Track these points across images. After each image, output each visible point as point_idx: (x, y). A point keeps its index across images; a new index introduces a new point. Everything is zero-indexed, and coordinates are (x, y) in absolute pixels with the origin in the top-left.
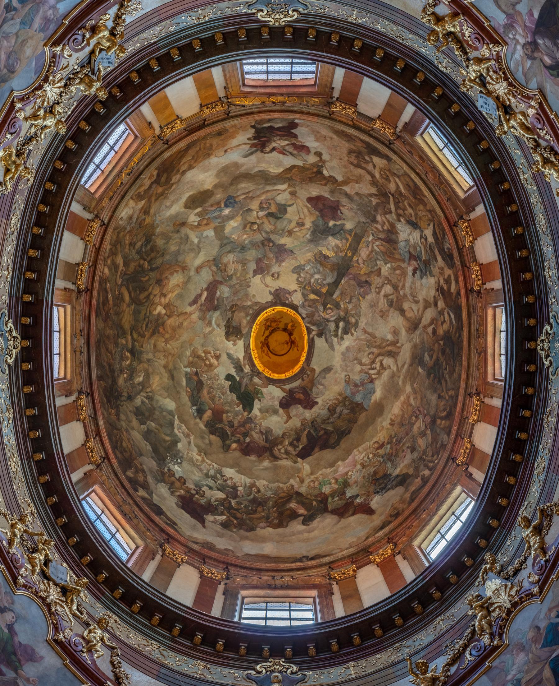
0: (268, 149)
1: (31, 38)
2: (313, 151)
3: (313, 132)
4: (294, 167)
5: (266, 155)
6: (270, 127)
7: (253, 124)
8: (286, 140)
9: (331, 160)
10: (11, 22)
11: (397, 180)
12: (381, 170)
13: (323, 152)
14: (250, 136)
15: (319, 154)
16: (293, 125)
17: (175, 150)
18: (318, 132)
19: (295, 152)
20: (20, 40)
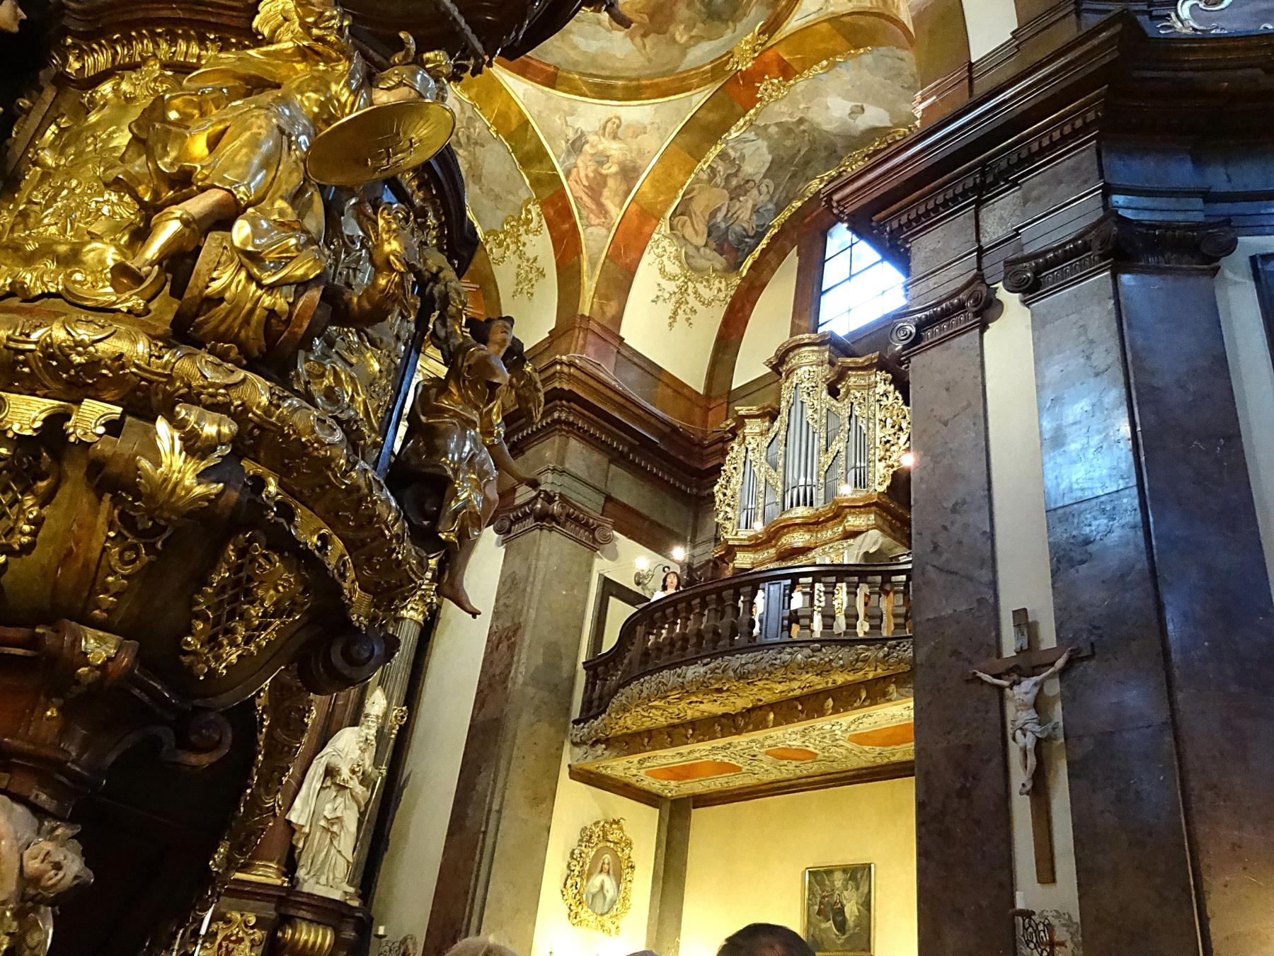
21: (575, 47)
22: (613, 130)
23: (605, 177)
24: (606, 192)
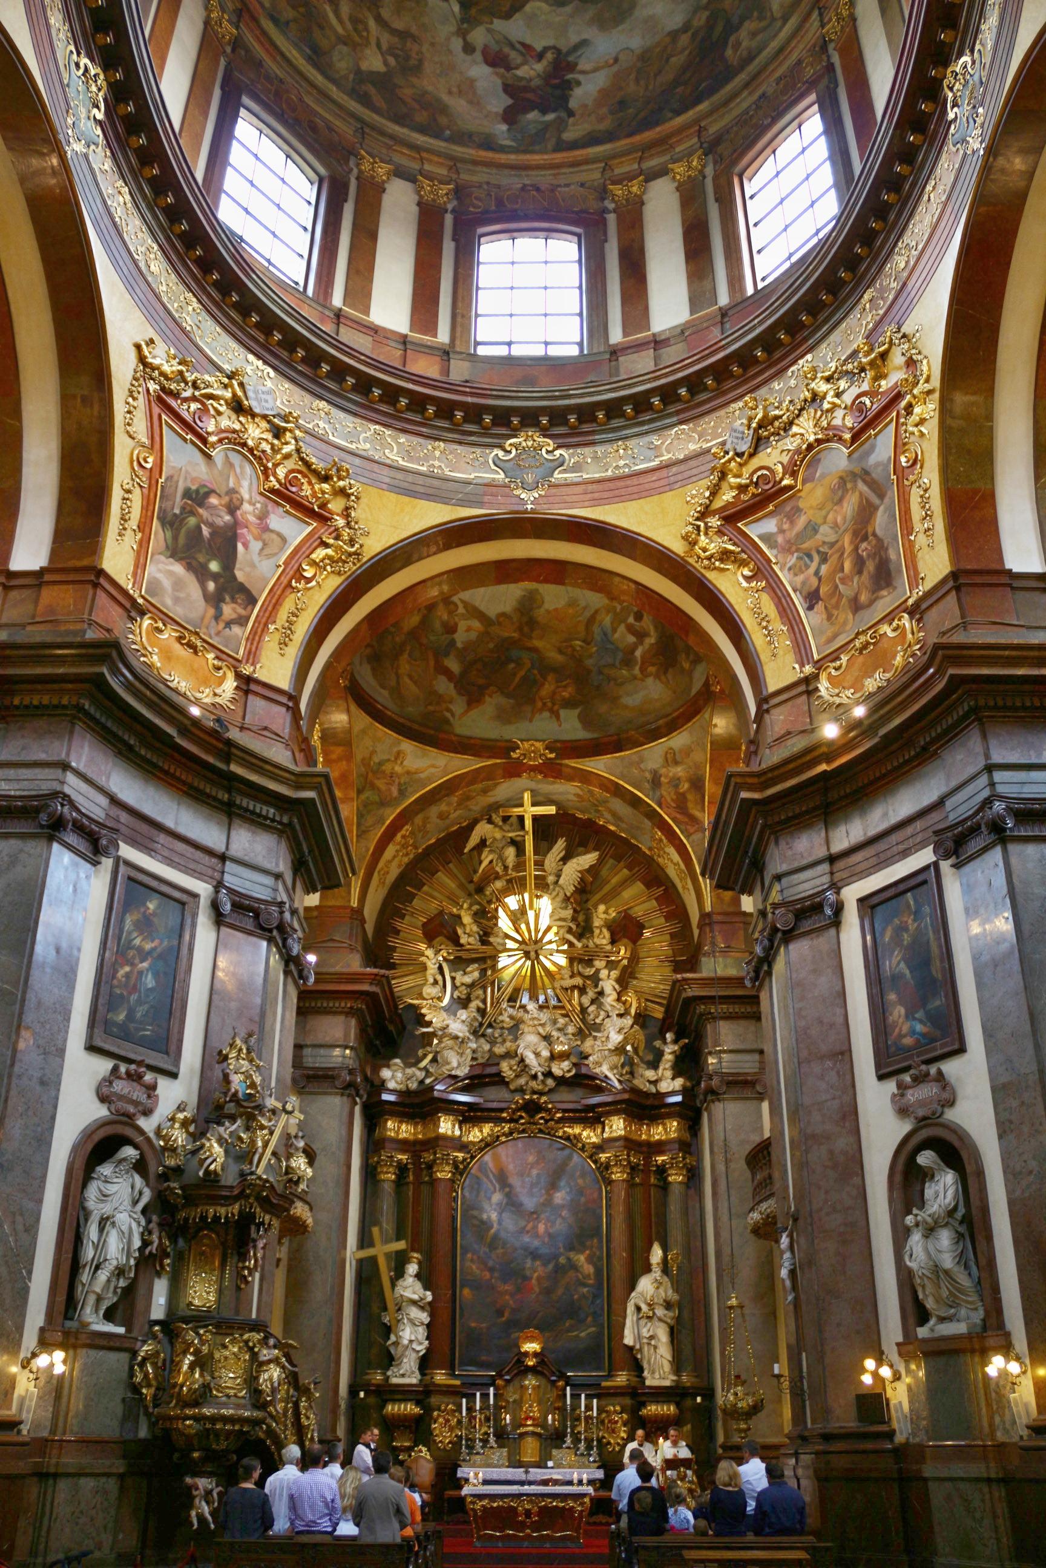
0: (550, 56)
1: (811, 507)
2: (478, 56)
3: (478, 103)
4: (508, 16)
5: (550, 42)
6: (544, 112)
7: (571, 120)
8: (522, 79)
9: (448, 39)
10: (827, 540)
11: (340, 30)
12: (367, 43)
13: (462, 55)
14: (578, 92)
15: (468, 49)
16: (510, 116)
17: (691, 113)
18: (471, 102)
19: (506, 50)
21: (626, 707)
22: (671, 758)
23: (683, 795)
24: (690, 805)
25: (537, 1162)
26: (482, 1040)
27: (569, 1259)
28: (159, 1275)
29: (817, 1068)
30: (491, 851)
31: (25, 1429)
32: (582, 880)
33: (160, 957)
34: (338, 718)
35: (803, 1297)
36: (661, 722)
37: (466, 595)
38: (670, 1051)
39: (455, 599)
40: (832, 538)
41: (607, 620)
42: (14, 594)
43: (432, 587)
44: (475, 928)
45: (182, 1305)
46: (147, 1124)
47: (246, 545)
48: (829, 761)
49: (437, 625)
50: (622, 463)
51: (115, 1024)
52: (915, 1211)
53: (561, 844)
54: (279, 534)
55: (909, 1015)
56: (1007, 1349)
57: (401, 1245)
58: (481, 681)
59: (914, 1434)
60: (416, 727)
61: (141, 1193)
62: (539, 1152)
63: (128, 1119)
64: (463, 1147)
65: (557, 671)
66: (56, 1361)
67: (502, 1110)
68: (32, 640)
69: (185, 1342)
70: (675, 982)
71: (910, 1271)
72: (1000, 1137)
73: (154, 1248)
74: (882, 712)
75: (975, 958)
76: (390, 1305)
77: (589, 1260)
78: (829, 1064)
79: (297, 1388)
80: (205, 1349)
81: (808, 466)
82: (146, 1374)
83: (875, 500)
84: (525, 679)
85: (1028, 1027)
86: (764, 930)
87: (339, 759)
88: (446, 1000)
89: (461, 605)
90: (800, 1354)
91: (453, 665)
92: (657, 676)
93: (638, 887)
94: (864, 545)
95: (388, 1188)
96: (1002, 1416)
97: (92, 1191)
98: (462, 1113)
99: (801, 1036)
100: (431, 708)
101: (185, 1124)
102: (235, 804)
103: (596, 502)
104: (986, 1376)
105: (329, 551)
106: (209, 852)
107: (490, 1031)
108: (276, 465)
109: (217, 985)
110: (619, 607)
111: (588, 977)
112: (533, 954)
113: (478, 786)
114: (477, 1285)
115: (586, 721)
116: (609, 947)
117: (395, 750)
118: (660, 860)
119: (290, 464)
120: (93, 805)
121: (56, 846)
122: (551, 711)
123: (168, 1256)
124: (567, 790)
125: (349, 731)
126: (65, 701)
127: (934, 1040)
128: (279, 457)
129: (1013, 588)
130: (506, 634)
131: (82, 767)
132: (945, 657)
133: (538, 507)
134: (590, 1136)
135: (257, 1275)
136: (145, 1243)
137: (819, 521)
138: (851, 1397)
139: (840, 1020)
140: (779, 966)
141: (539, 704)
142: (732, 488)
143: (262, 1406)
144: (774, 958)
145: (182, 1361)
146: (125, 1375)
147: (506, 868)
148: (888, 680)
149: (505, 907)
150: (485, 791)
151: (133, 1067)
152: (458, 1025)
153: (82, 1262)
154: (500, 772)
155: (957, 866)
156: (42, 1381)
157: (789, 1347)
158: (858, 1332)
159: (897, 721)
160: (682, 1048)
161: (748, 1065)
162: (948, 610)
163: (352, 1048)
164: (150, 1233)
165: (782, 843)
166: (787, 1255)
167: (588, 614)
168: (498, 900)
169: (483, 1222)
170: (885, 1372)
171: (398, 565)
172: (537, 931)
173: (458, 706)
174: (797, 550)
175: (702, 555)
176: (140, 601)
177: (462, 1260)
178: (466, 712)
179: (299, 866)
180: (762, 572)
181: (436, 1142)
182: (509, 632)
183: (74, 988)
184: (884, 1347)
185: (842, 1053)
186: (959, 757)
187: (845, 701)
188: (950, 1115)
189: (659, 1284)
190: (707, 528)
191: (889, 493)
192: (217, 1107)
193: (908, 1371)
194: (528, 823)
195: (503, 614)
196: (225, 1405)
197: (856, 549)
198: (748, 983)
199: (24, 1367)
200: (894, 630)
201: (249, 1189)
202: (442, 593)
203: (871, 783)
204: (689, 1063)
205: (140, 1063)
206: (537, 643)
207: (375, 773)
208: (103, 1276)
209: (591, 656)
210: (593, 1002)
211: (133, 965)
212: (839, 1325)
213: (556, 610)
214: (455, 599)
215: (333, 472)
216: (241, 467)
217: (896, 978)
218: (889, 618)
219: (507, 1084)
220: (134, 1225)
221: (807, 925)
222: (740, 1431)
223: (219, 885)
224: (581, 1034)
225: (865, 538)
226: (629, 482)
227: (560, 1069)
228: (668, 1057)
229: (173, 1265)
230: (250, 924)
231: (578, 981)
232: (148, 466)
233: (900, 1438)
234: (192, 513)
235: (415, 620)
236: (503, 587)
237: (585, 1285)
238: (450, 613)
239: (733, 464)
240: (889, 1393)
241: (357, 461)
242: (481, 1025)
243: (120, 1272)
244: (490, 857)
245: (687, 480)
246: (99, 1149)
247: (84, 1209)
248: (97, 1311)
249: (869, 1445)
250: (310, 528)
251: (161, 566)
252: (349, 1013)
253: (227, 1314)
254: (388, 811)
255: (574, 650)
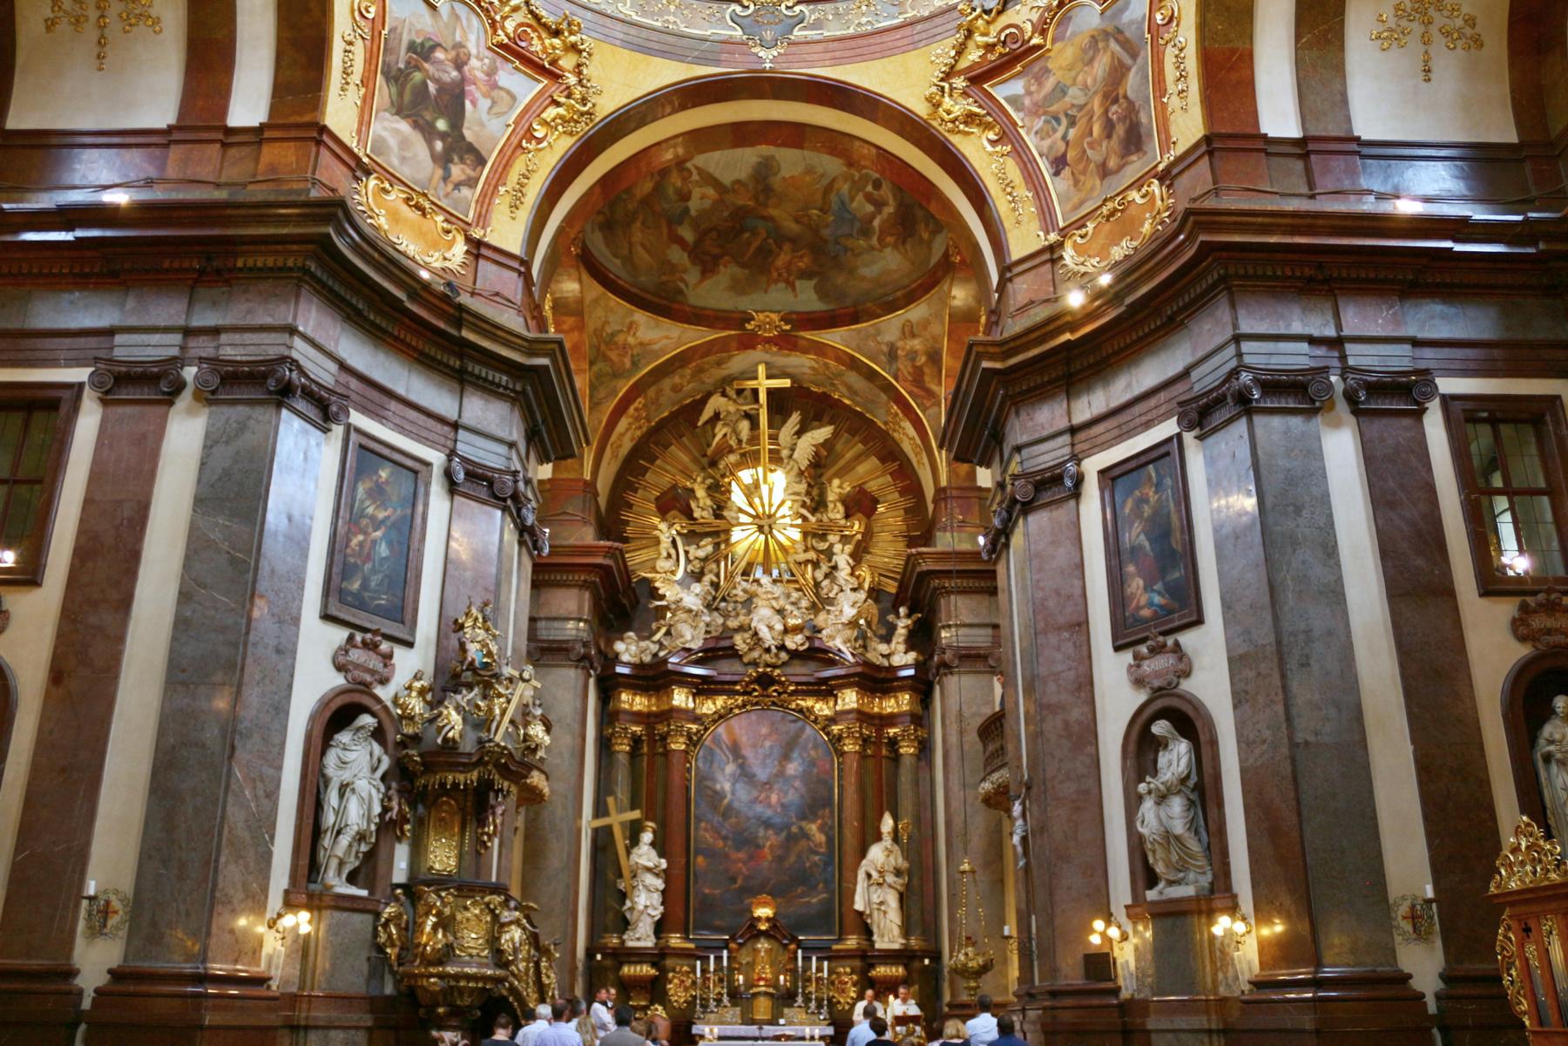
1: (1061, 68)
10: (1075, 102)
20: (1073, 73)
21: (863, 279)
22: (909, 331)
24: (927, 379)
25: (770, 734)
26: (716, 614)
27: (801, 828)
28: (399, 840)
29: (1053, 639)
30: (725, 425)
31: (274, 985)
32: (817, 454)
33: (394, 524)
34: (570, 287)
35: (1032, 861)
36: (899, 294)
37: (700, 160)
38: (903, 624)
39: (689, 165)
40: (1081, 101)
41: (845, 188)
42: (233, 152)
43: (667, 150)
44: (709, 502)
45: (423, 870)
46: (384, 693)
47: (474, 103)
48: (1072, 331)
49: (671, 191)
50: (864, 20)
51: (351, 593)
52: (1148, 779)
53: (795, 418)
54: (508, 92)
55: (1148, 587)
56: (1233, 909)
57: (636, 814)
58: (716, 251)
59: (1139, 991)
60: (649, 297)
61: (379, 761)
62: (772, 724)
63: (365, 688)
64: (697, 719)
65: (793, 240)
66: (302, 921)
67: (735, 683)
68: (254, 199)
69: (427, 904)
70: (909, 556)
71: (1141, 837)
72: (1235, 707)
73: (394, 814)
74: (1129, 280)
75: (1217, 530)
76: (626, 872)
77: (821, 829)
78: (1066, 635)
79: (537, 948)
80: (447, 911)
81: (1058, 24)
82: (390, 935)
83: (1127, 60)
84: (760, 250)
85: (1267, 599)
86: (1002, 502)
87: (572, 330)
88: (680, 574)
89: (695, 172)
90: (1029, 917)
91: (687, 234)
92: (895, 247)
93: (873, 461)
94: (1114, 108)
95: (623, 759)
96: (1225, 973)
97: (331, 758)
98: (696, 686)
99: (1038, 607)
100: (664, 278)
101: (422, 692)
102: (466, 371)
103: (837, 61)
104: (1212, 938)
105: (561, 111)
106: (442, 420)
107: (723, 604)
108: (504, 18)
109: (452, 555)
110: (857, 175)
111: (821, 552)
112: (766, 529)
113: (712, 358)
114: (710, 853)
115: (822, 293)
116: (843, 522)
117: (628, 320)
118: (896, 435)
119: (520, 17)
120: (322, 371)
121: (285, 412)
122: (787, 282)
123: (408, 821)
124: (803, 363)
125: (580, 301)
126: (290, 263)
127: (1171, 612)
128: (507, 9)
129: (1268, 154)
130: (741, 203)
131: (309, 332)
132: (1196, 223)
133: (777, 66)
134: (822, 708)
135: (496, 841)
136: (386, 810)
137: (1069, 82)
138: (1080, 957)
139: (1078, 592)
140: (1017, 540)
141: (775, 275)
142: (978, 47)
143: (505, 965)
144: (1012, 531)
145: (424, 923)
146: (369, 936)
147: (740, 441)
148: (1135, 249)
149: (738, 480)
150: (719, 364)
151: (369, 636)
152: (692, 598)
153: (324, 827)
154: (734, 344)
155: (1200, 438)
156: (289, 941)
157: (1018, 911)
158: (1088, 895)
159: (1144, 290)
160: (915, 623)
161: (981, 638)
162: (1198, 178)
163: (586, 621)
164: (390, 799)
165: (1023, 415)
166: (1019, 822)
167: (825, 182)
168: (732, 474)
169: (716, 792)
170: (1114, 932)
171: (633, 125)
172: (771, 505)
173: (693, 276)
174: (1045, 113)
175: (946, 117)
176: (366, 160)
177: (696, 829)
178: (701, 281)
179: (532, 436)
180: (1008, 135)
181: (670, 714)
182: (744, 200)
183: (306, 556)
184: (1113, 910)
185: (1079, 625)
186: (1207, 327)
187: (1090, 269)
188: (1186, 686)
189: (889, 852)
190: (952, 89)
191: (1142, 53)
192: (455, 675)
193: (1135, 932)
194: (763, 397)
195: (738, 182)
196: (468, 964)
197: (1106, 111)
198: (985, 556)
199: (270, 927)
200: (1143, 197)
201: (487, 756)
202: (677, 156)
203: (1115, 353)
204: (922, 637)
205: (376, 632)
206: (774, 212)
207: (607, 344)
208: (344, 841)
209: (827, 226)
210: (826, 576)
211: (366, 533)
212: (1069, 888)
213: (792, 177)
214: (689, 165)
215: (564, 26)
216: (468, 20)
217: (1135, 550)
218: (1138, 184)
219: (740, 657)
220: (374, 792)
221: (1046, 497)
222: (970, 988)
223: (452, 454)
224: (814, 608)
225: (1116, 101)
226: (871, 41)
227: (793, 642)
228: (901, 632)
229: (413, 831)
230: (483, 493)
231: (812, 555)
232: (370, 16)
233: (1125, 994)
234: (418, 68)
235: (648, 186)
236: (739, 151)
237: (816, 853)
238: (684, 179)
239: (980, 22)
240: (1117, 952)
241: (589, 15)
242: (715, 598)
243: (361, 837)
244: (725, 430)
245: (932, 39)
246: (337, 717)
247: (324, 775)
248: (339, 874)
249: (1095, 1001)
250: (541, 86)
251: (386, 124)
252: (583, 586)
253: (468, 877)
254: (621, 382)
255: (809, 217)
